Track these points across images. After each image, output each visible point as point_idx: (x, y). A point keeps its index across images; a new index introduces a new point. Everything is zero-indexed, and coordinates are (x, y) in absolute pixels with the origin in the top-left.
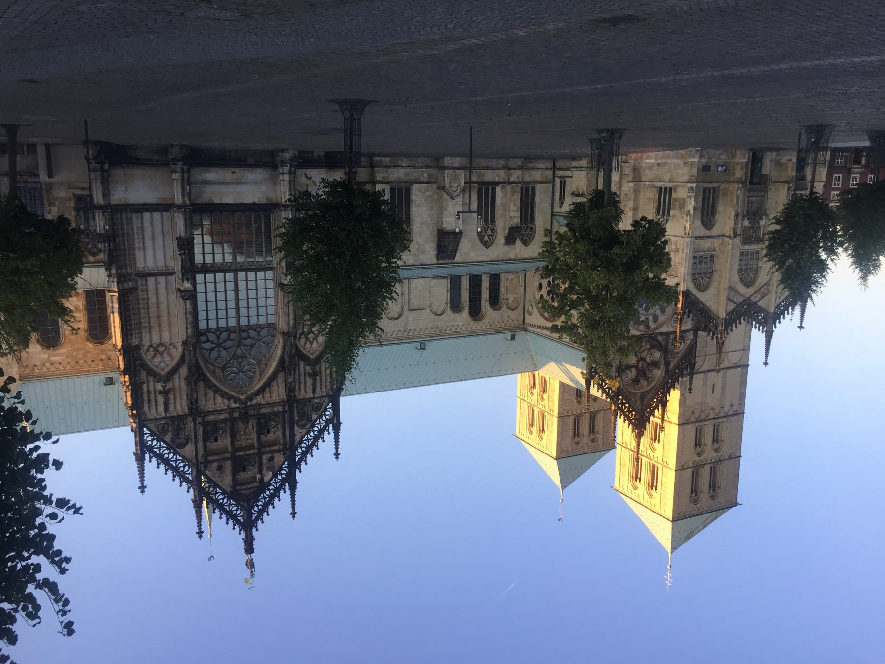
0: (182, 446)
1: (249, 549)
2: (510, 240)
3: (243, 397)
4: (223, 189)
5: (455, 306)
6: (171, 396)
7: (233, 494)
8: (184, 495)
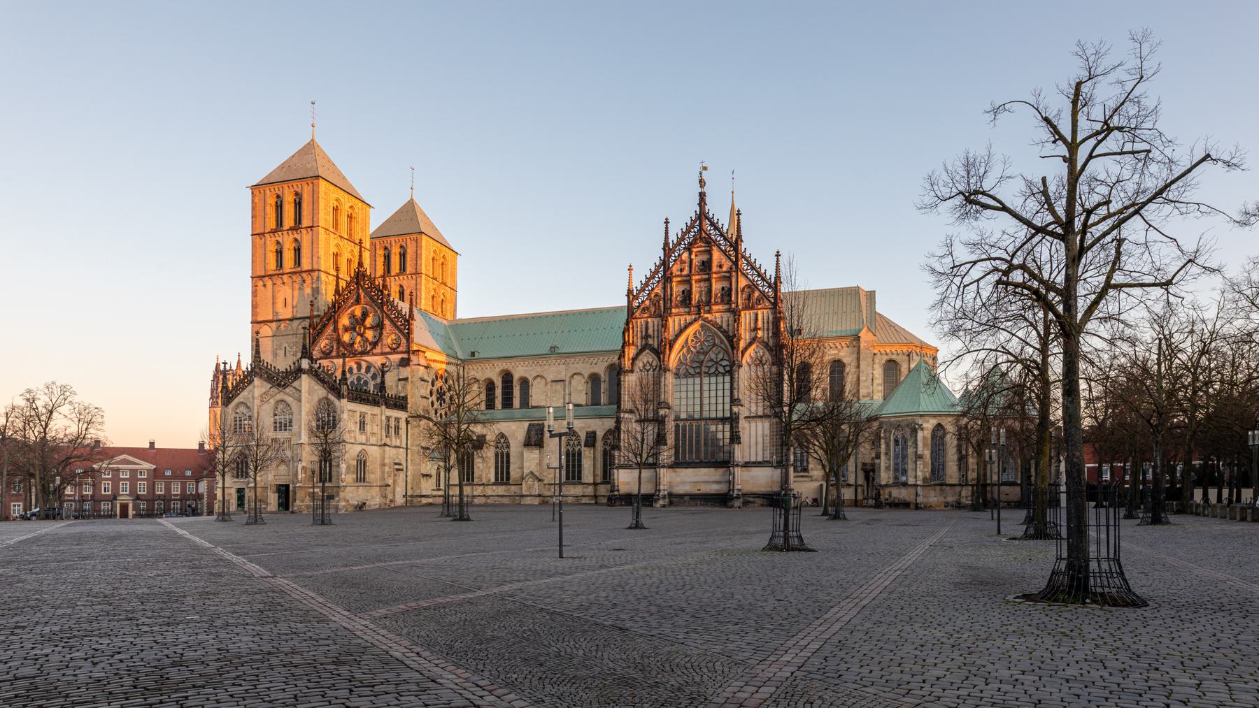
0: (748, 286)
4: (707, 478)
5: (525, 383)
8: (748, 246)
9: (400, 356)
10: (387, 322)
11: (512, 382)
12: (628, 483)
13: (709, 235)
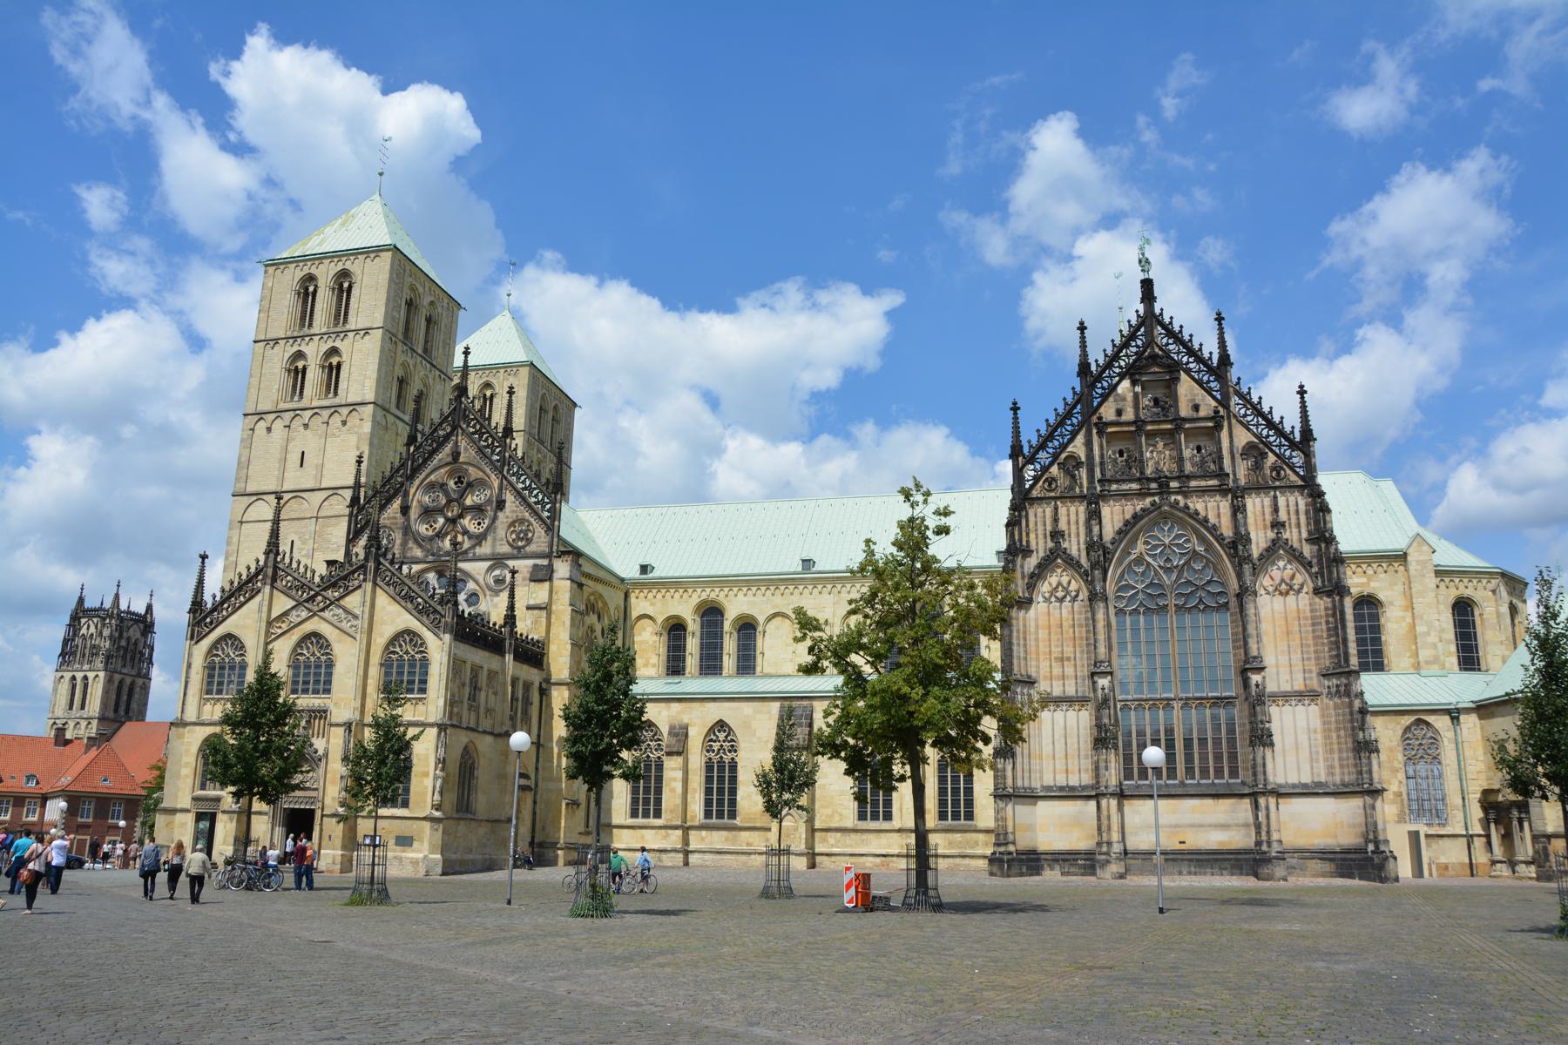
1: (1147, 285)
2: (680, 733)
4: (1197, 818)
5: (747, 628)
6: (1269, 518)
7: (1174, 369)
9: (531, 562)
10: (509, 497)
12: (1031, 828)
13: (1167, 354)
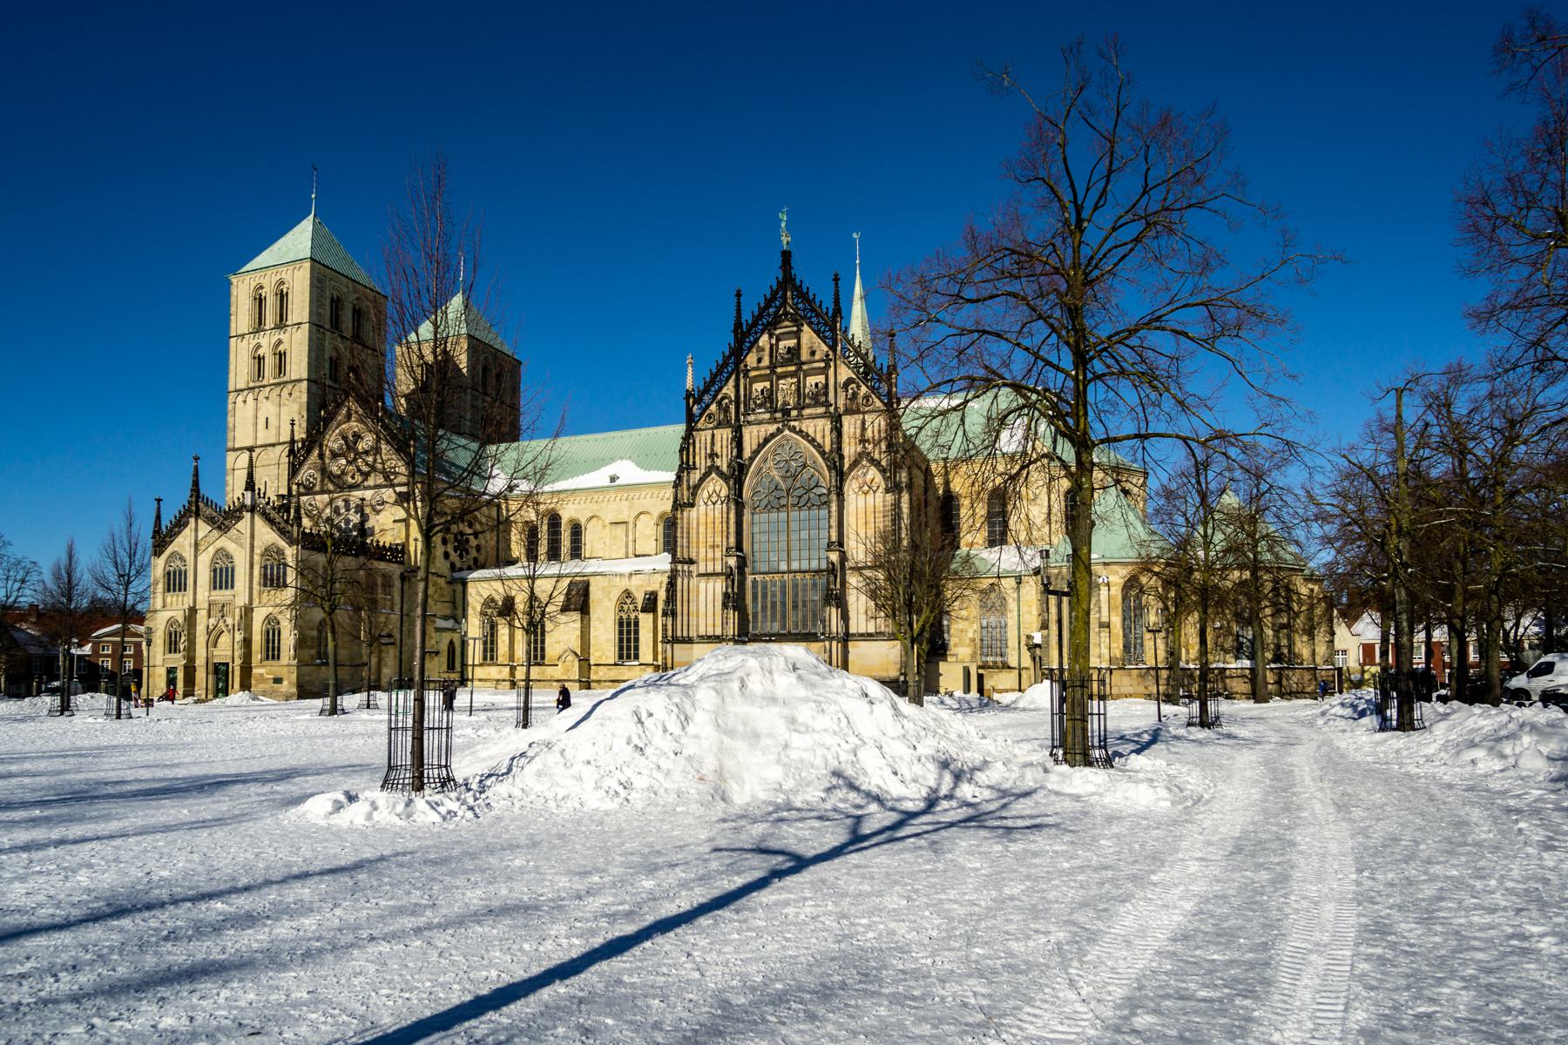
0: (850, 381)
3: (787, 432)
11: (559, 525)
